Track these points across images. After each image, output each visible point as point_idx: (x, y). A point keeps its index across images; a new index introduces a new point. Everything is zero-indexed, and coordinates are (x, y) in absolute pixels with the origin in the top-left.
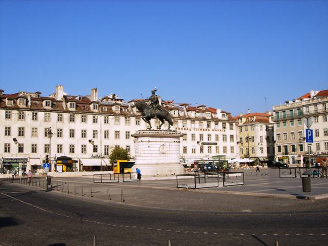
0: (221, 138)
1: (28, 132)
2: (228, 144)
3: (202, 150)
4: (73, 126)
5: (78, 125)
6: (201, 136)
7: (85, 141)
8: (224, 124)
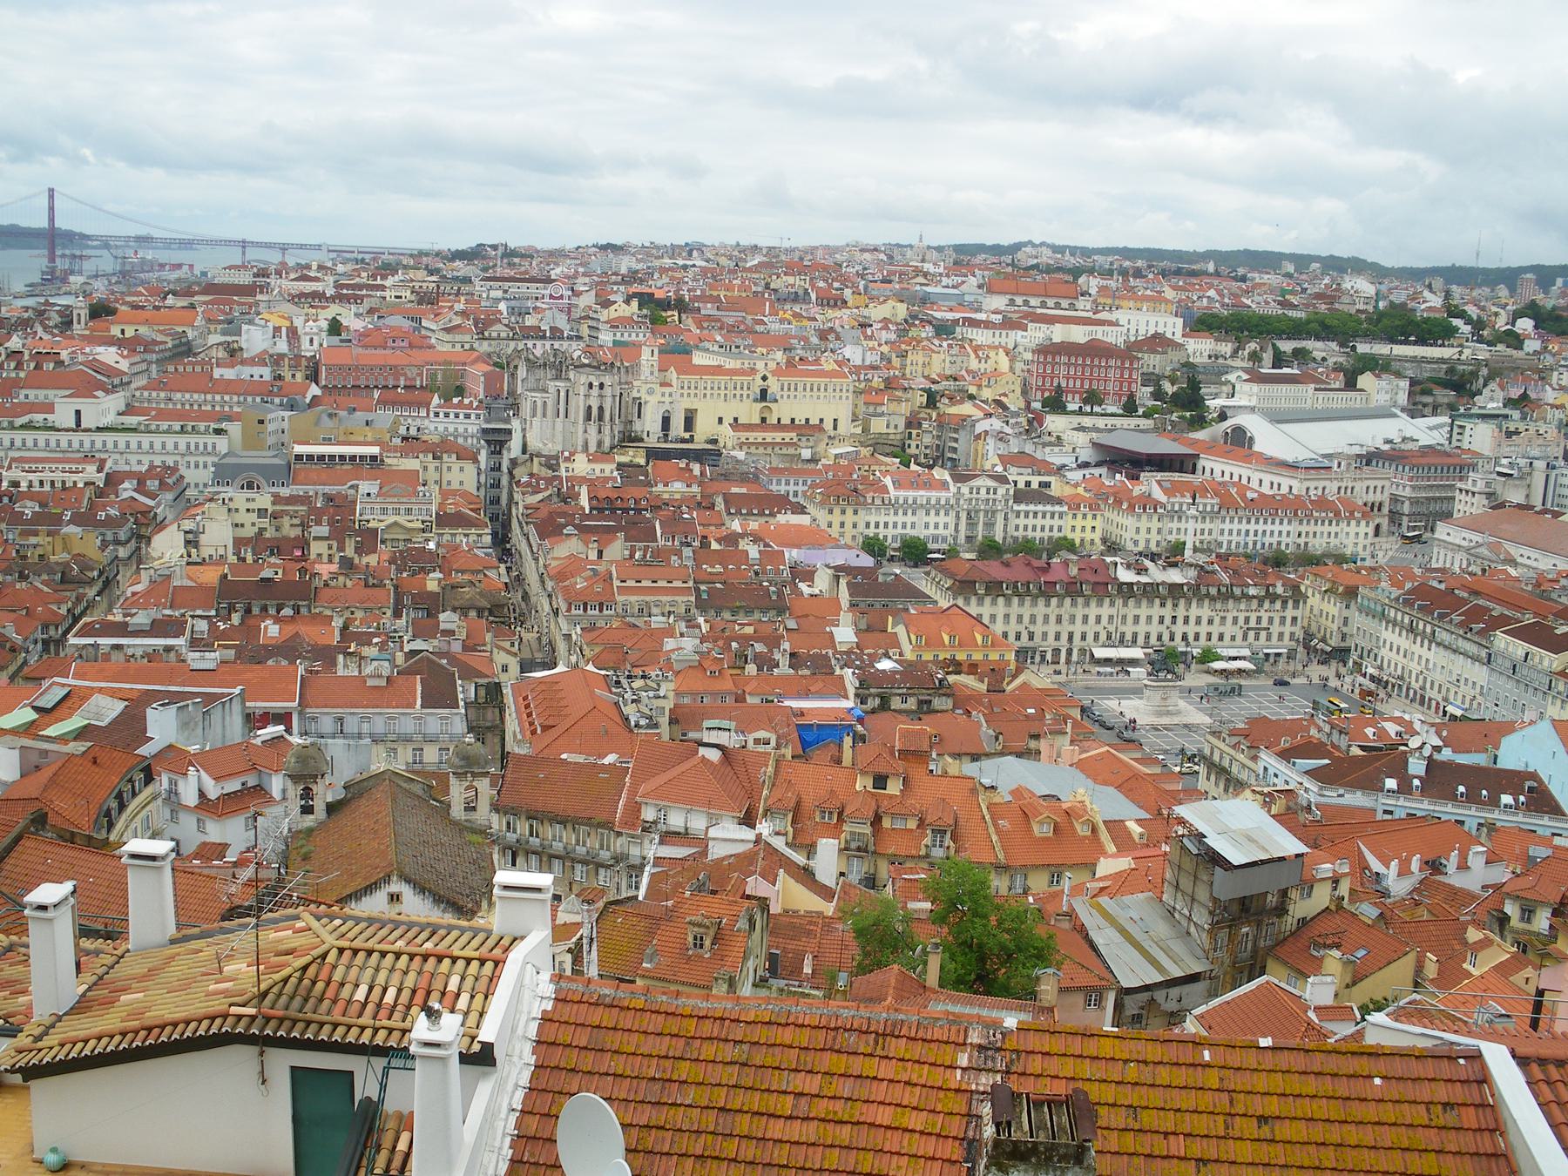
0: (1277, 621)
1: (1040, 619)
2: (1288, 629)
3: (1245, 638)
4: (1086, 611)
5: (1093, 611)
6: (1247, 620)
7: (1099, 628)
8: (1285, 603)
